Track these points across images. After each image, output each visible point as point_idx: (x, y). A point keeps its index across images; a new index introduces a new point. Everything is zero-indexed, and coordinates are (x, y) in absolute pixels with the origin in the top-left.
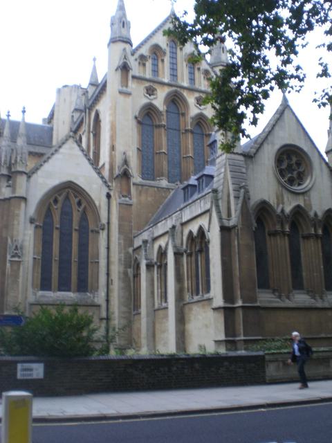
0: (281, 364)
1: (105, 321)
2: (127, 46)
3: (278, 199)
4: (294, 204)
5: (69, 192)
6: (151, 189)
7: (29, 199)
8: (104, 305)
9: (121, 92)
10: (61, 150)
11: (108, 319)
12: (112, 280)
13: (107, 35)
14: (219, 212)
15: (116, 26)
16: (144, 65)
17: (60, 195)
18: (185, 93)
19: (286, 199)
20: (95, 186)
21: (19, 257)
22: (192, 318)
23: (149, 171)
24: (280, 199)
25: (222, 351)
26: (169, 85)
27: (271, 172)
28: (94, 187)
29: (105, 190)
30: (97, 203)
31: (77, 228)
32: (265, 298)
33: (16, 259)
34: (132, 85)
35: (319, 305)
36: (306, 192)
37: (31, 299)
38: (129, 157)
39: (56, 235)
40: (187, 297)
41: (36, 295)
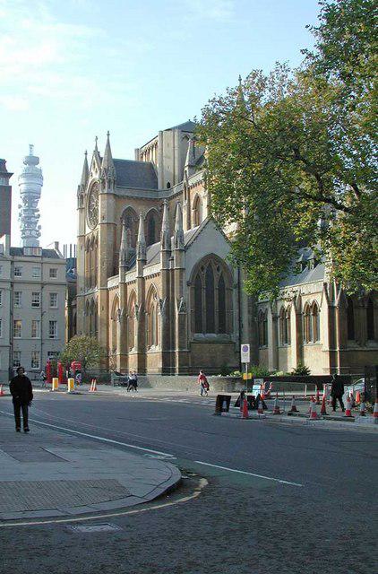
14: (327, 294)
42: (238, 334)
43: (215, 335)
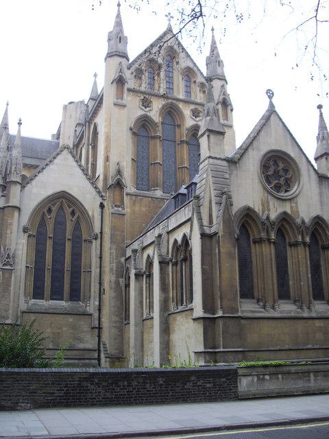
0: (256, 379)
1: (97, 330)
2: (123, 60)
3: (263, 205)
4: (280, 210)
5: (62, 201)
6: (145, 199)
7: (23, 208)
8: (96, 315)
9: (115, 104)
10: (56, 161)
11: (100, 328)
12: (104, 289)
13: (104, 49)
14: (200, 219)
15: (112, 42)
16: (140, 78)
17: (54, 205)
18: (181, 105)
19: (271, 206)
20: (88, 196)
21: (11, 265)
22: (176, 328)
23: (144, 181)
24: (265, 205)
25: (200, 363)
26: (163, 96)
27: (257, 181)
28: (88, 198)
29: (99, 200)
30: (90, 213)
31: (70, 237)
32: (248, 308)
33: (8, 267)
34: (128, 98)
35: (305, 315)
36: (293, 198)
37: (23, 307)
38: (123, 167)
39: (49, 244)
40: (172, 308)
41: (28, 303)
42: (97, 303)
43: (63, 303)
